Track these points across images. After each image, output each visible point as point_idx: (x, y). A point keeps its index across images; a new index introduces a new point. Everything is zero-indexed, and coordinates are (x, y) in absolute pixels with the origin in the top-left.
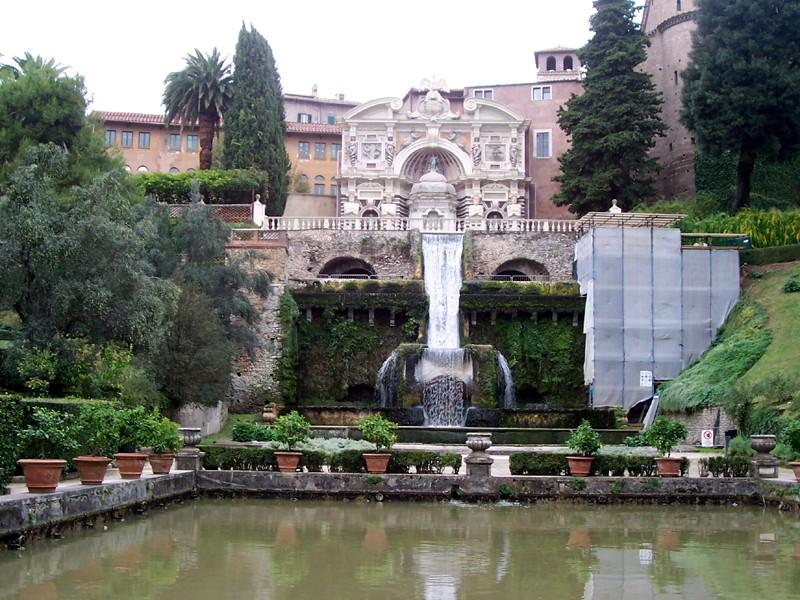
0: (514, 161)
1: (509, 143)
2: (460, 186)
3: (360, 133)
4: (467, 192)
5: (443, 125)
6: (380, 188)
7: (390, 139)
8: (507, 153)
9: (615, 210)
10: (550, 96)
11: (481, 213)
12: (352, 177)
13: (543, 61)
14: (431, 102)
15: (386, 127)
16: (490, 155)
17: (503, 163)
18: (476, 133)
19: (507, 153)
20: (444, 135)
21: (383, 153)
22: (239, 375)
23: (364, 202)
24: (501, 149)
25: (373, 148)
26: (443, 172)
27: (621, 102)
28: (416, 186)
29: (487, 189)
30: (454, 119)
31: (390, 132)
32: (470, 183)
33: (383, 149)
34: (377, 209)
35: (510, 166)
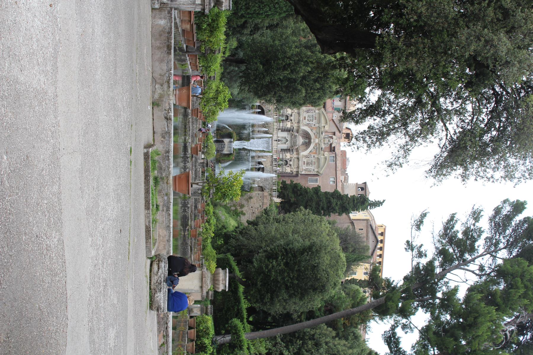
0: (306, 170)
1: (313, 168)
2: (297, 150)
4: (295, 153)
6: (297, 121)
7: (314, 125)
9: (278, 200)
10: (331, 183)
11: (287, 158)
13: (363, 186)
18: (316, 156)
19: (309, 167)
20: (316, 144)
21: (308, 122)
23: (291, 115)
26: (303, 144)
28: (297, 134)
29: (296, 160)
31: (317, 125)
32: (298, 154)
33: (311, 122)
34: (289, 120)
35: (304, 168)
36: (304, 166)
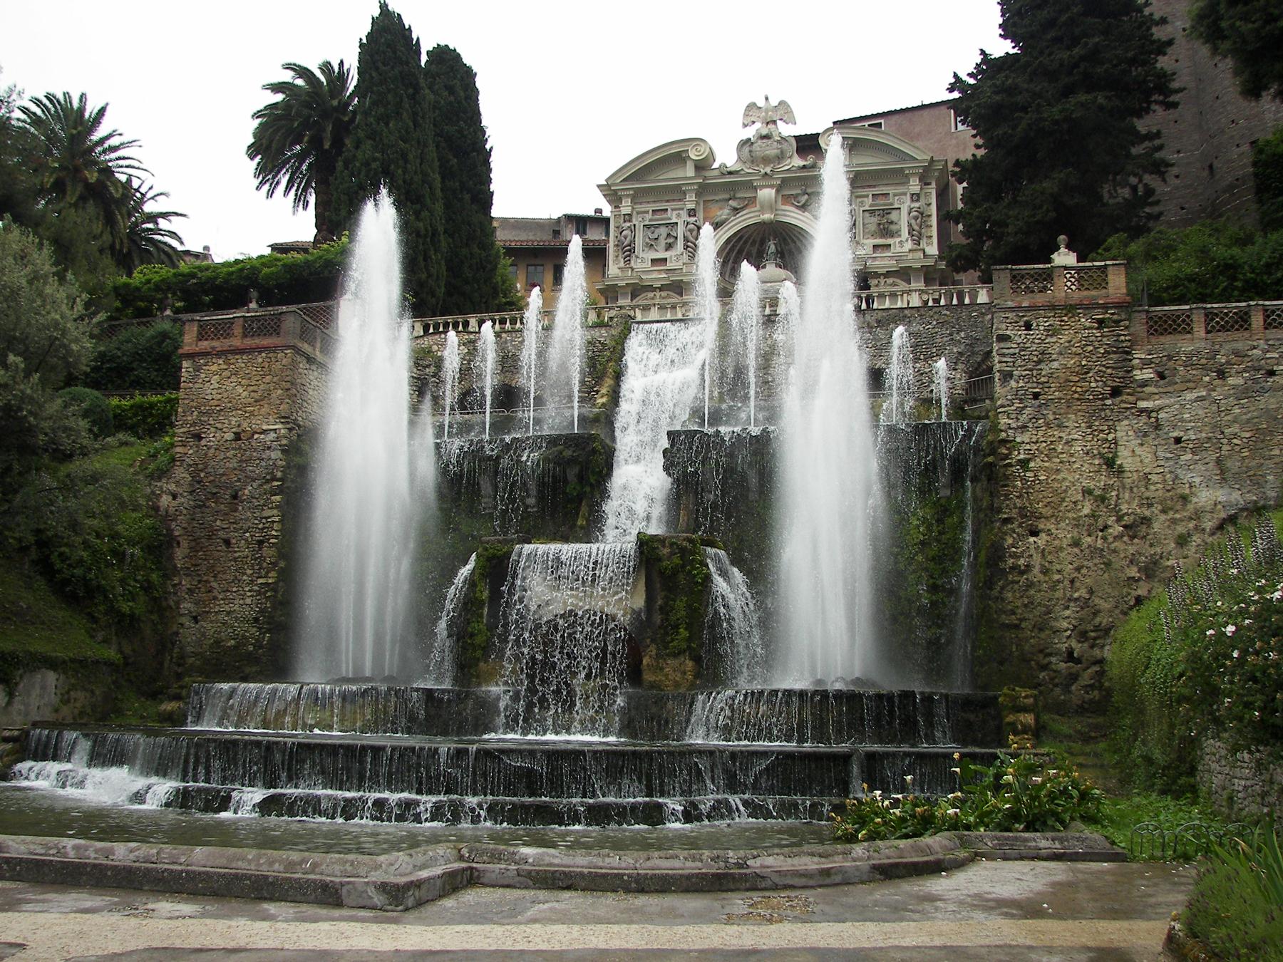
1: (906, 204)
3: (639, 208)
5: (784, 180)
8: (903, 221)
12: (623, 283)
14: (760, 142)
15: (684, 193)
16: (873, 227)
17: (898, 240)
19: (903, 221)
20: (787, 199)
22: (196, 619)
24: (894, 216)
25: (663, 231)
27: (1075, 41)
30: (804, 167)
31: (690, 201)
33: (680, 231)
35: (909, 245)
36: (896, 249)
